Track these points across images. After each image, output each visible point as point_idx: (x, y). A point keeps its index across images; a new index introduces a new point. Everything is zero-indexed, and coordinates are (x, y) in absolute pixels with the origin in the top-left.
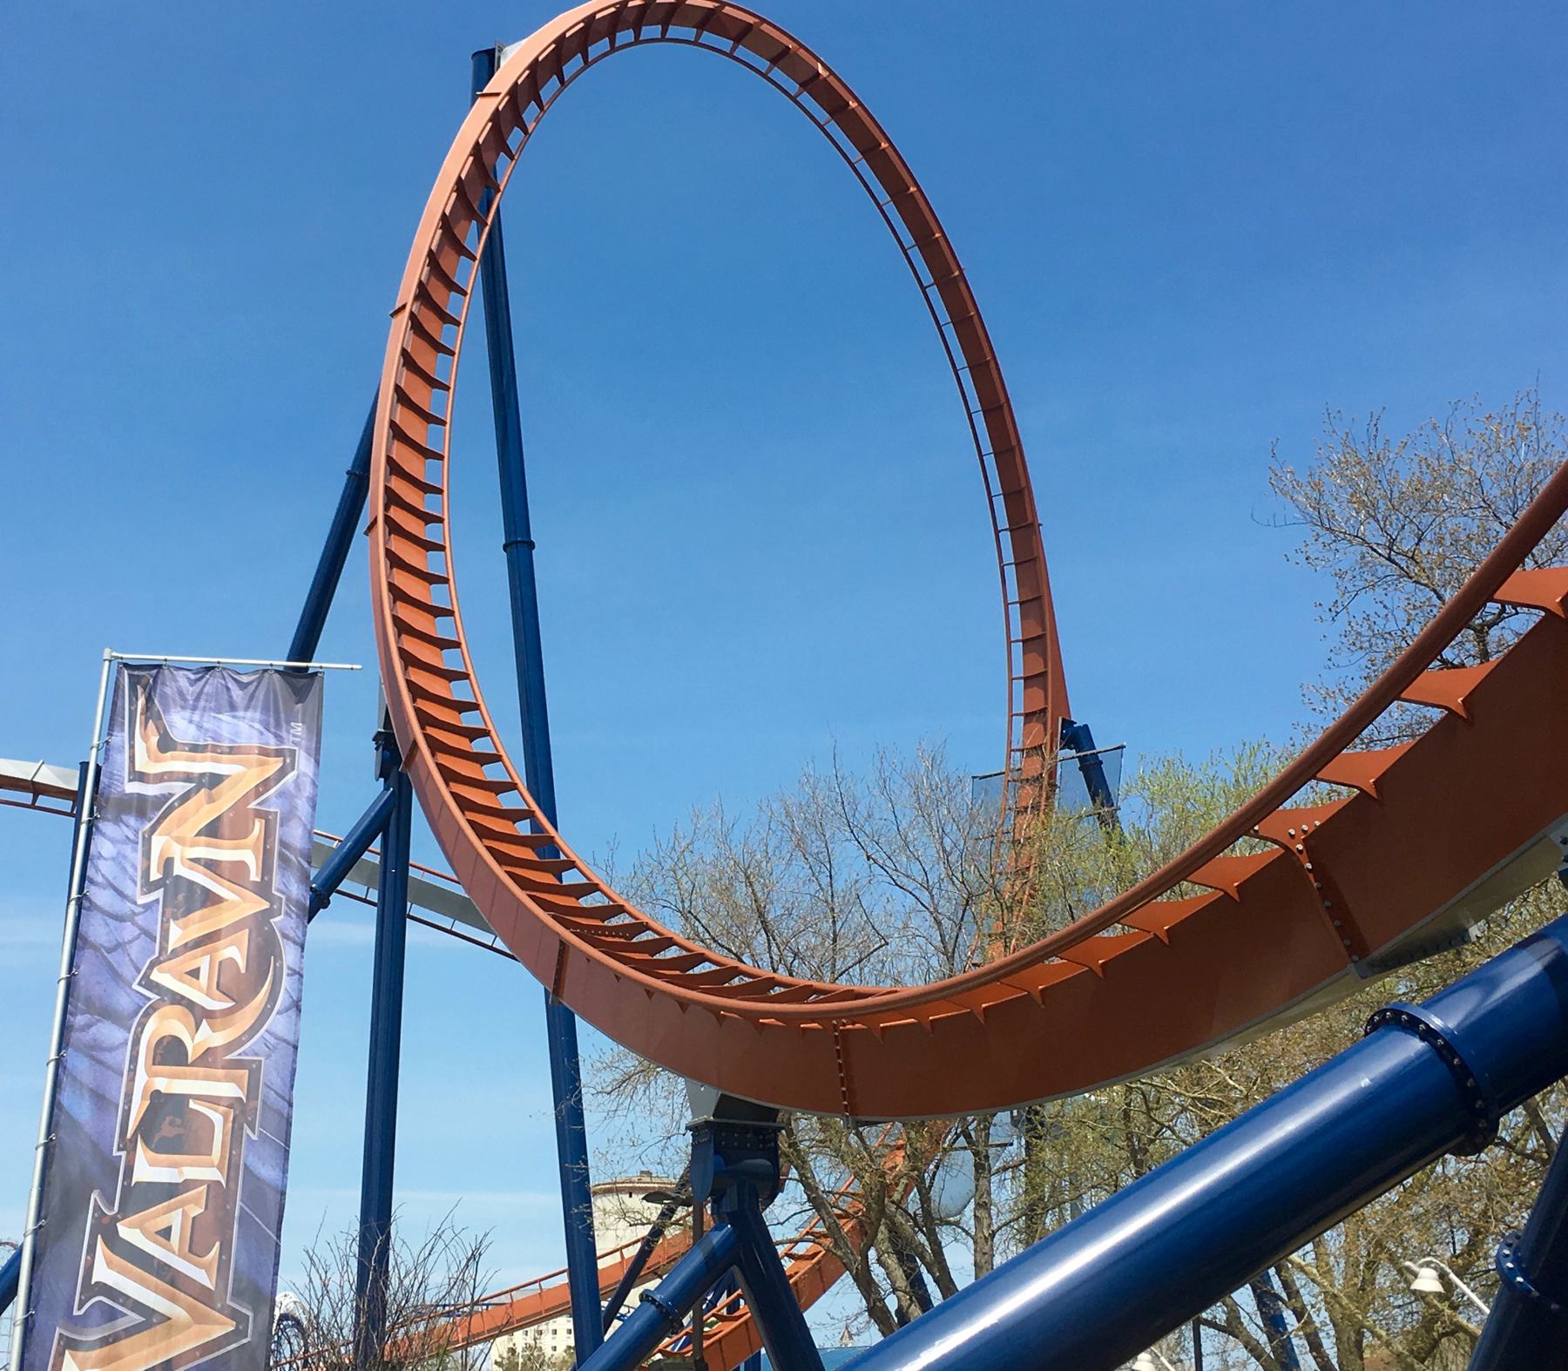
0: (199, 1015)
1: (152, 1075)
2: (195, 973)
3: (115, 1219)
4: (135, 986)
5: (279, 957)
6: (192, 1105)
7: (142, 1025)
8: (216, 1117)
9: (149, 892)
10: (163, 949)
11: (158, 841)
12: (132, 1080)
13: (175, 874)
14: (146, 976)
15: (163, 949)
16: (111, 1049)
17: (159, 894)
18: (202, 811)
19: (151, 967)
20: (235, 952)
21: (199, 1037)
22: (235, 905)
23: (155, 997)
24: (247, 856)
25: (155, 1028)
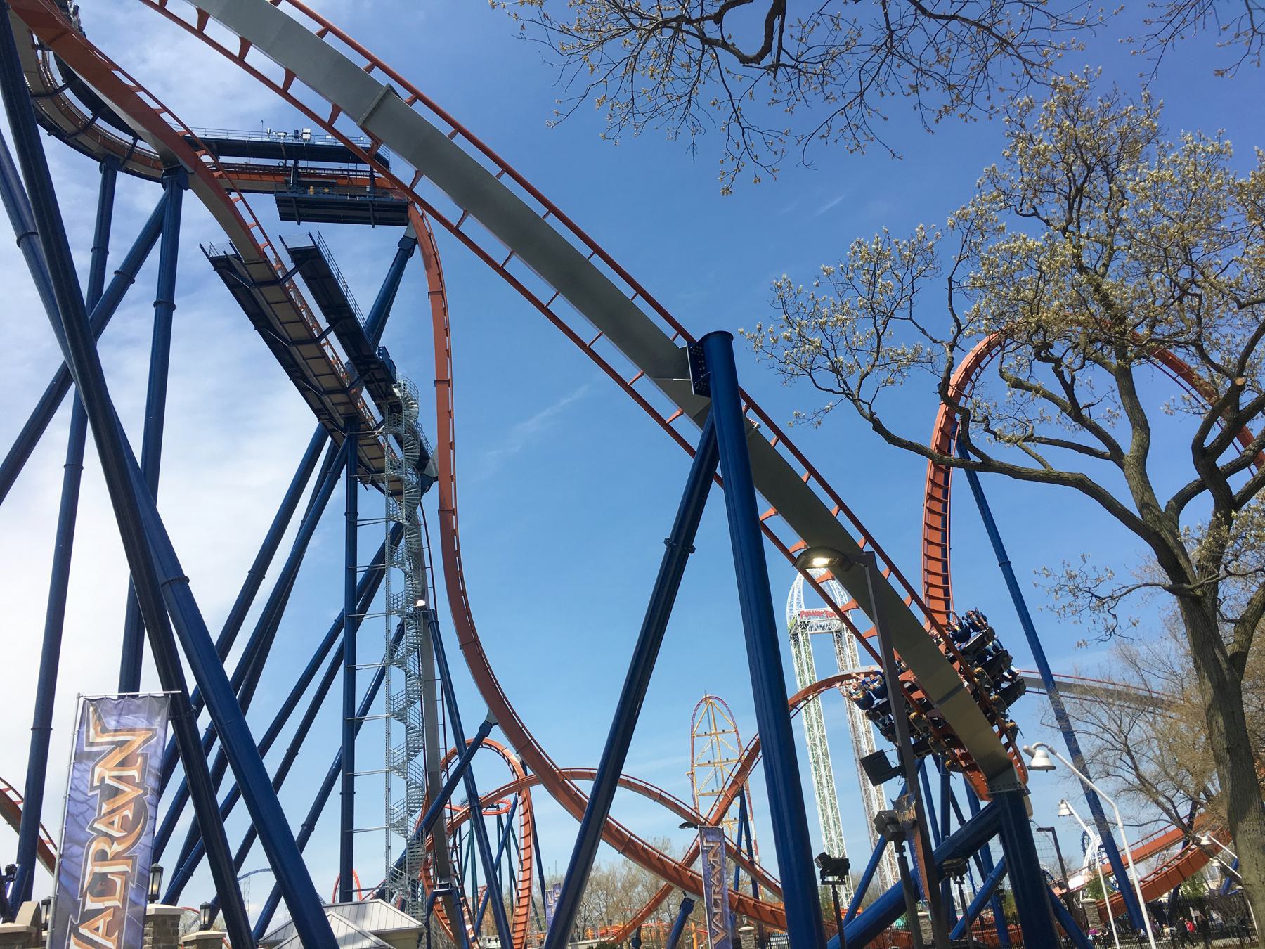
0: (112, 839)
1: (93, 866)
2: (112, 823)
3: (78, 925)
4: (87, 830)
5: (146, 812)
6: (109, 876)
7: (90, 846)
8: (118, 881)
9: (94, 790)
10: (99, 814)
11: (98, 770)
12: (85, 868)
13: (106, 782)
14: (92, 825)
15: (99, 814)
16: (77, 857)
17: (98, 792)
18: (119, 757)
19: (94, 821)
20: (128, 813)
21: (113, 849)
22: (129, 793)
23: (95, 834)
24: (134, 773)
25: (95, 847)
